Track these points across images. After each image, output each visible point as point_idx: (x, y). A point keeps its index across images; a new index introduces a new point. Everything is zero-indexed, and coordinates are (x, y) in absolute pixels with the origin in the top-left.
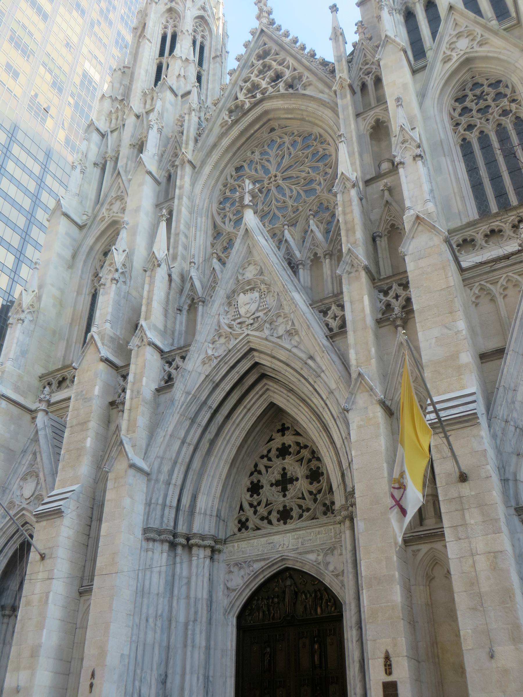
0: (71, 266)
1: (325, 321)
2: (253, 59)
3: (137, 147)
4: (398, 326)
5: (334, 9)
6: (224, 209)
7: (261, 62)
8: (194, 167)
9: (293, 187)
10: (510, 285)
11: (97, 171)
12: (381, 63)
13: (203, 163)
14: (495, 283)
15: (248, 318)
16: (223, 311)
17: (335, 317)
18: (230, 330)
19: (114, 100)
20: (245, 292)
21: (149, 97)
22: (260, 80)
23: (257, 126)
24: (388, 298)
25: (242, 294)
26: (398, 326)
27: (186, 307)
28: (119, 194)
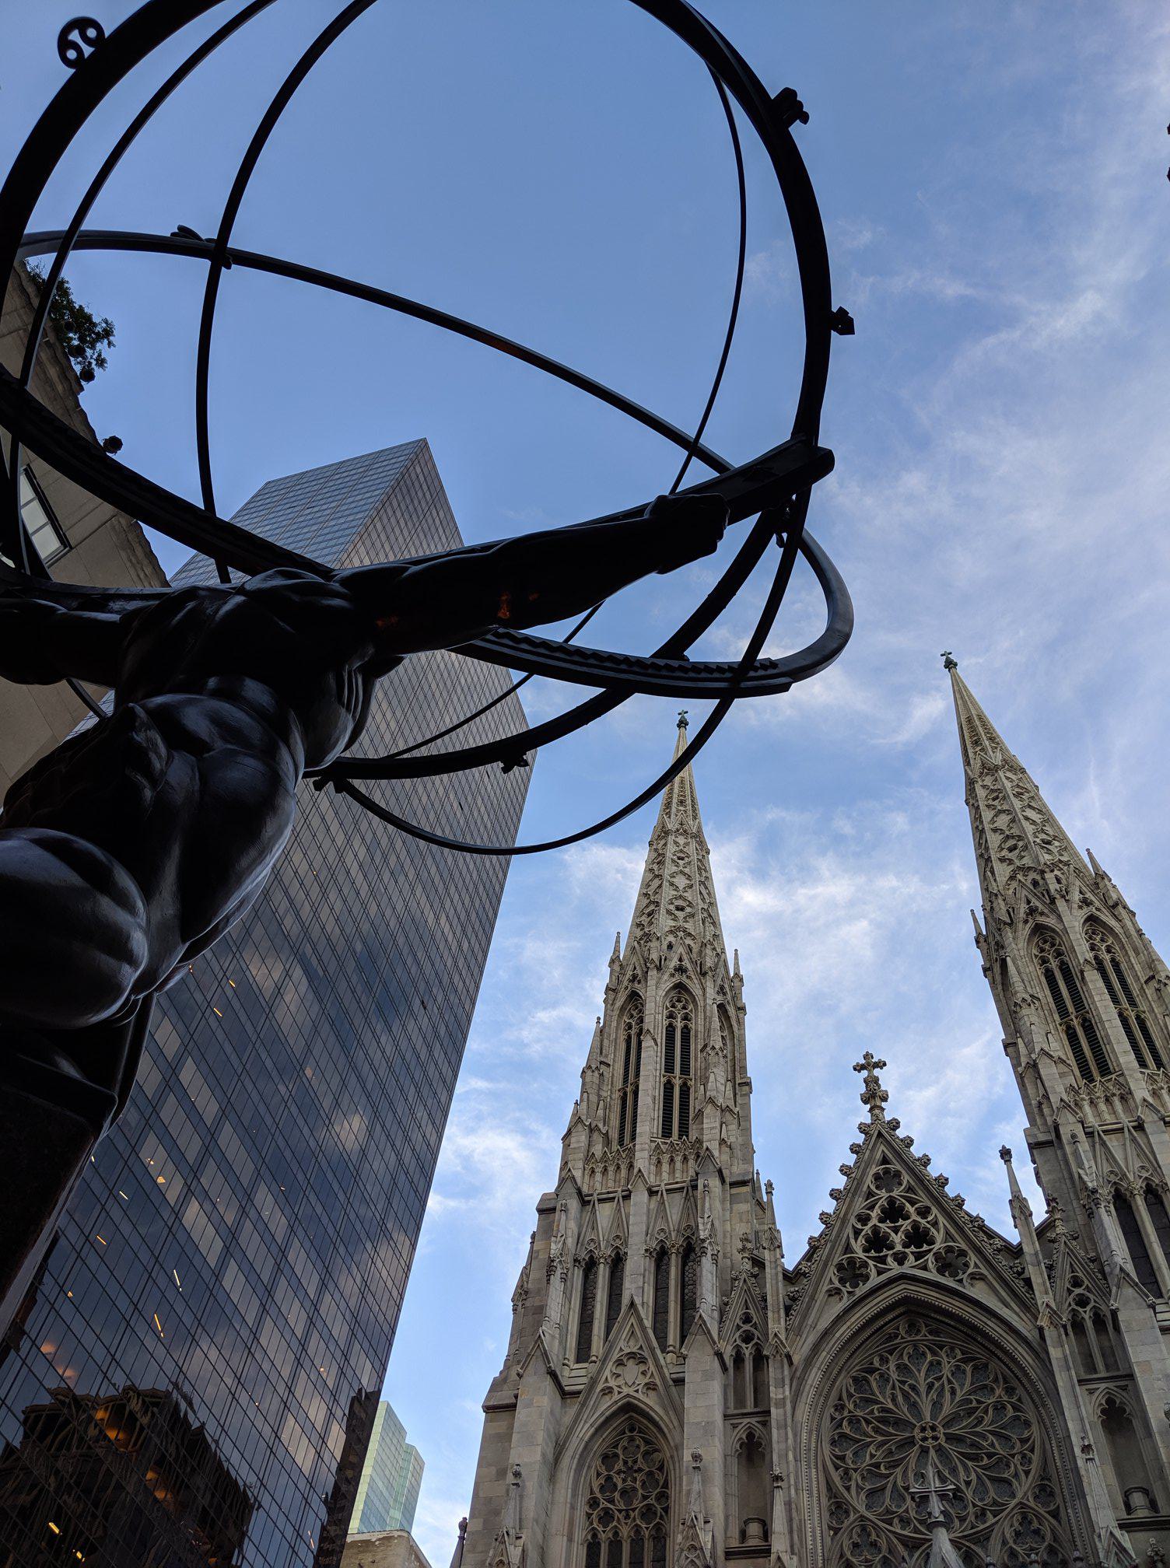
0: (552, 1478)
2: (869, 1181)
3: (654, 1254)
5: (1006, 1154)
6: (842, 1458)
7: (883, 1194)
8: (791, 1363)
9: (970, 1464)
11: (578, 1275)
12: (1121, 1317)
13: (809, 1362)
19: (592, 1130)
21: (666, 1158)
22: (889, 1231)
23: (890, 1316)
28: (634, 1350)
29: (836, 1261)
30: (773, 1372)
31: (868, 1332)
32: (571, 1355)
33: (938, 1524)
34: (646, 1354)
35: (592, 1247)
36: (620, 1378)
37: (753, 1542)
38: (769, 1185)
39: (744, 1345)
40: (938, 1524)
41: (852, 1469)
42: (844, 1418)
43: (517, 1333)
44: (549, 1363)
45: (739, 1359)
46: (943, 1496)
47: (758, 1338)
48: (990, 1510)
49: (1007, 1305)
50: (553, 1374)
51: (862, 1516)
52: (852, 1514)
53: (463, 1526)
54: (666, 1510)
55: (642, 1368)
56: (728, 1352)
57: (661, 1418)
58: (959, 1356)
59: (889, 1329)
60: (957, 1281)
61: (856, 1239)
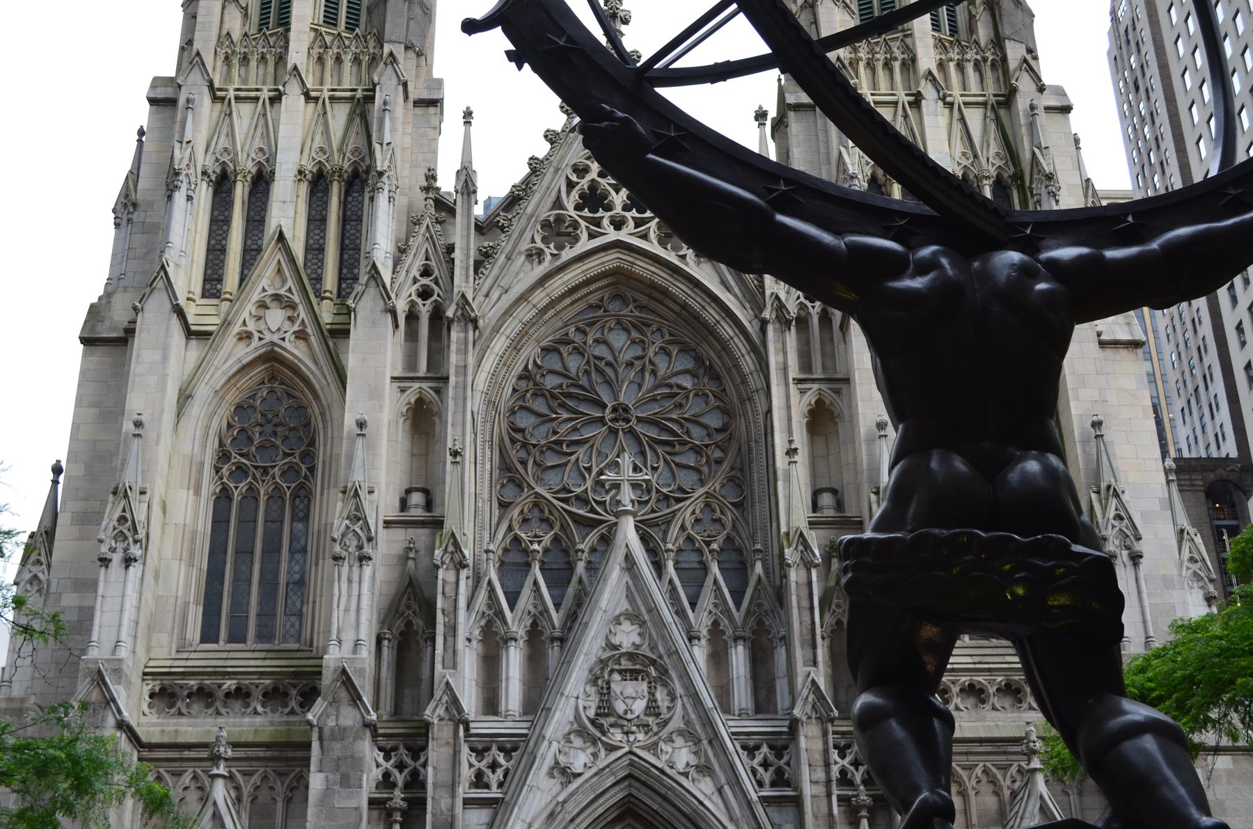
1: (752, 767)
4: (864, 817)
9: (660, 450)
10: (984, 779)
11: (204, 194)
13: (496, 330)
14: (970, 768)
15: (629, 721)
16: (582, 690)
17: (765, 764)
18: (599, 735)
20: (620, 672)
24: (846, 762)
25: (616, 677)
26: (864, 817)
27: (477, 632)
29: (543, 217)
30: (455, 334)
31: (568, 301)
32: (197, 287)
33: (627, 512)
34: (296, 298)
35: (226, 158)
36: (262, 321)
37: (417, 513)
38: (468, 114)
39: (419, 301)
40: (627, 512)
41: (532, 445)
42: (527, 391)
43: (121, 255)
44: (176, 299)
45: (412, 317)
46: (635, 486)
47: (439, 295)
48: (674, 498)
49: (728, 288)
50: (180, 312)
51: (536, 493)
52: (526, 490)
53: (57, 470)
54: (312, 470)
55: (290, 313)
56: (402, 306)
57: (312, 373)
58: (667, 337)
59: (593, 299)
60: (679, 256)
61: (568, 193)
